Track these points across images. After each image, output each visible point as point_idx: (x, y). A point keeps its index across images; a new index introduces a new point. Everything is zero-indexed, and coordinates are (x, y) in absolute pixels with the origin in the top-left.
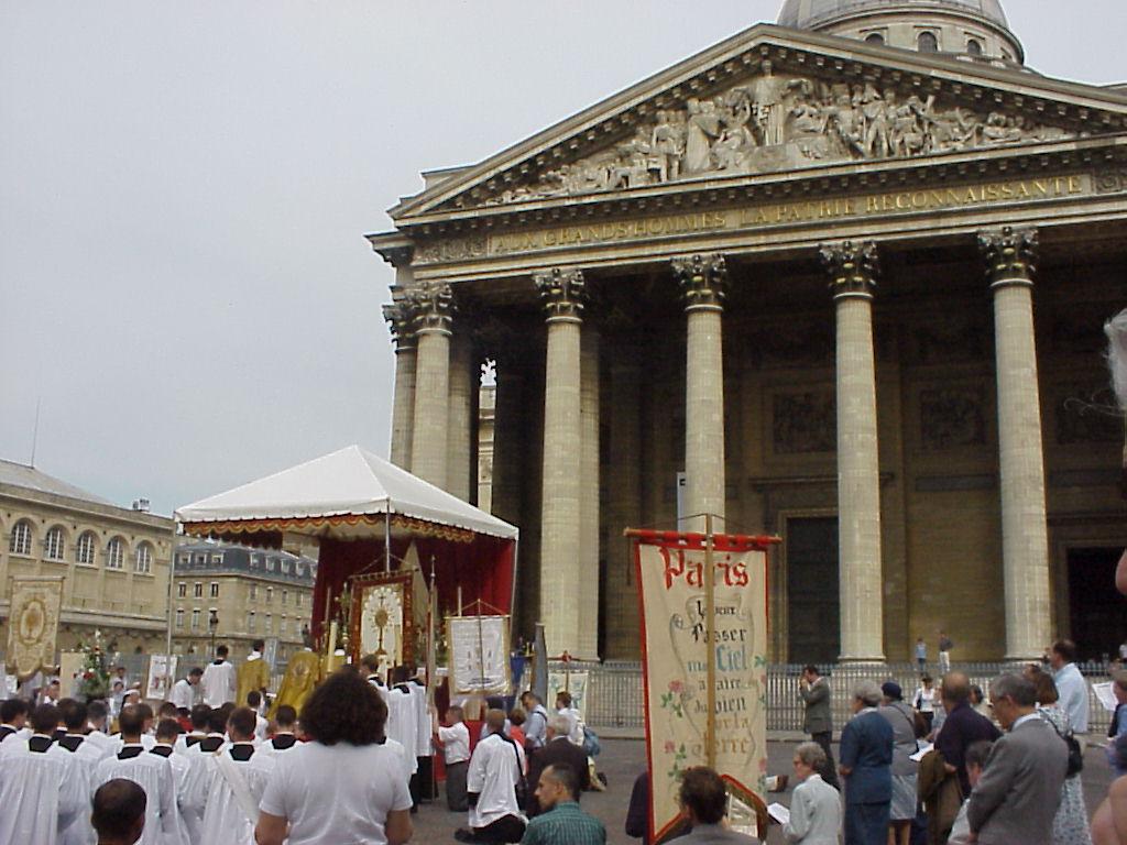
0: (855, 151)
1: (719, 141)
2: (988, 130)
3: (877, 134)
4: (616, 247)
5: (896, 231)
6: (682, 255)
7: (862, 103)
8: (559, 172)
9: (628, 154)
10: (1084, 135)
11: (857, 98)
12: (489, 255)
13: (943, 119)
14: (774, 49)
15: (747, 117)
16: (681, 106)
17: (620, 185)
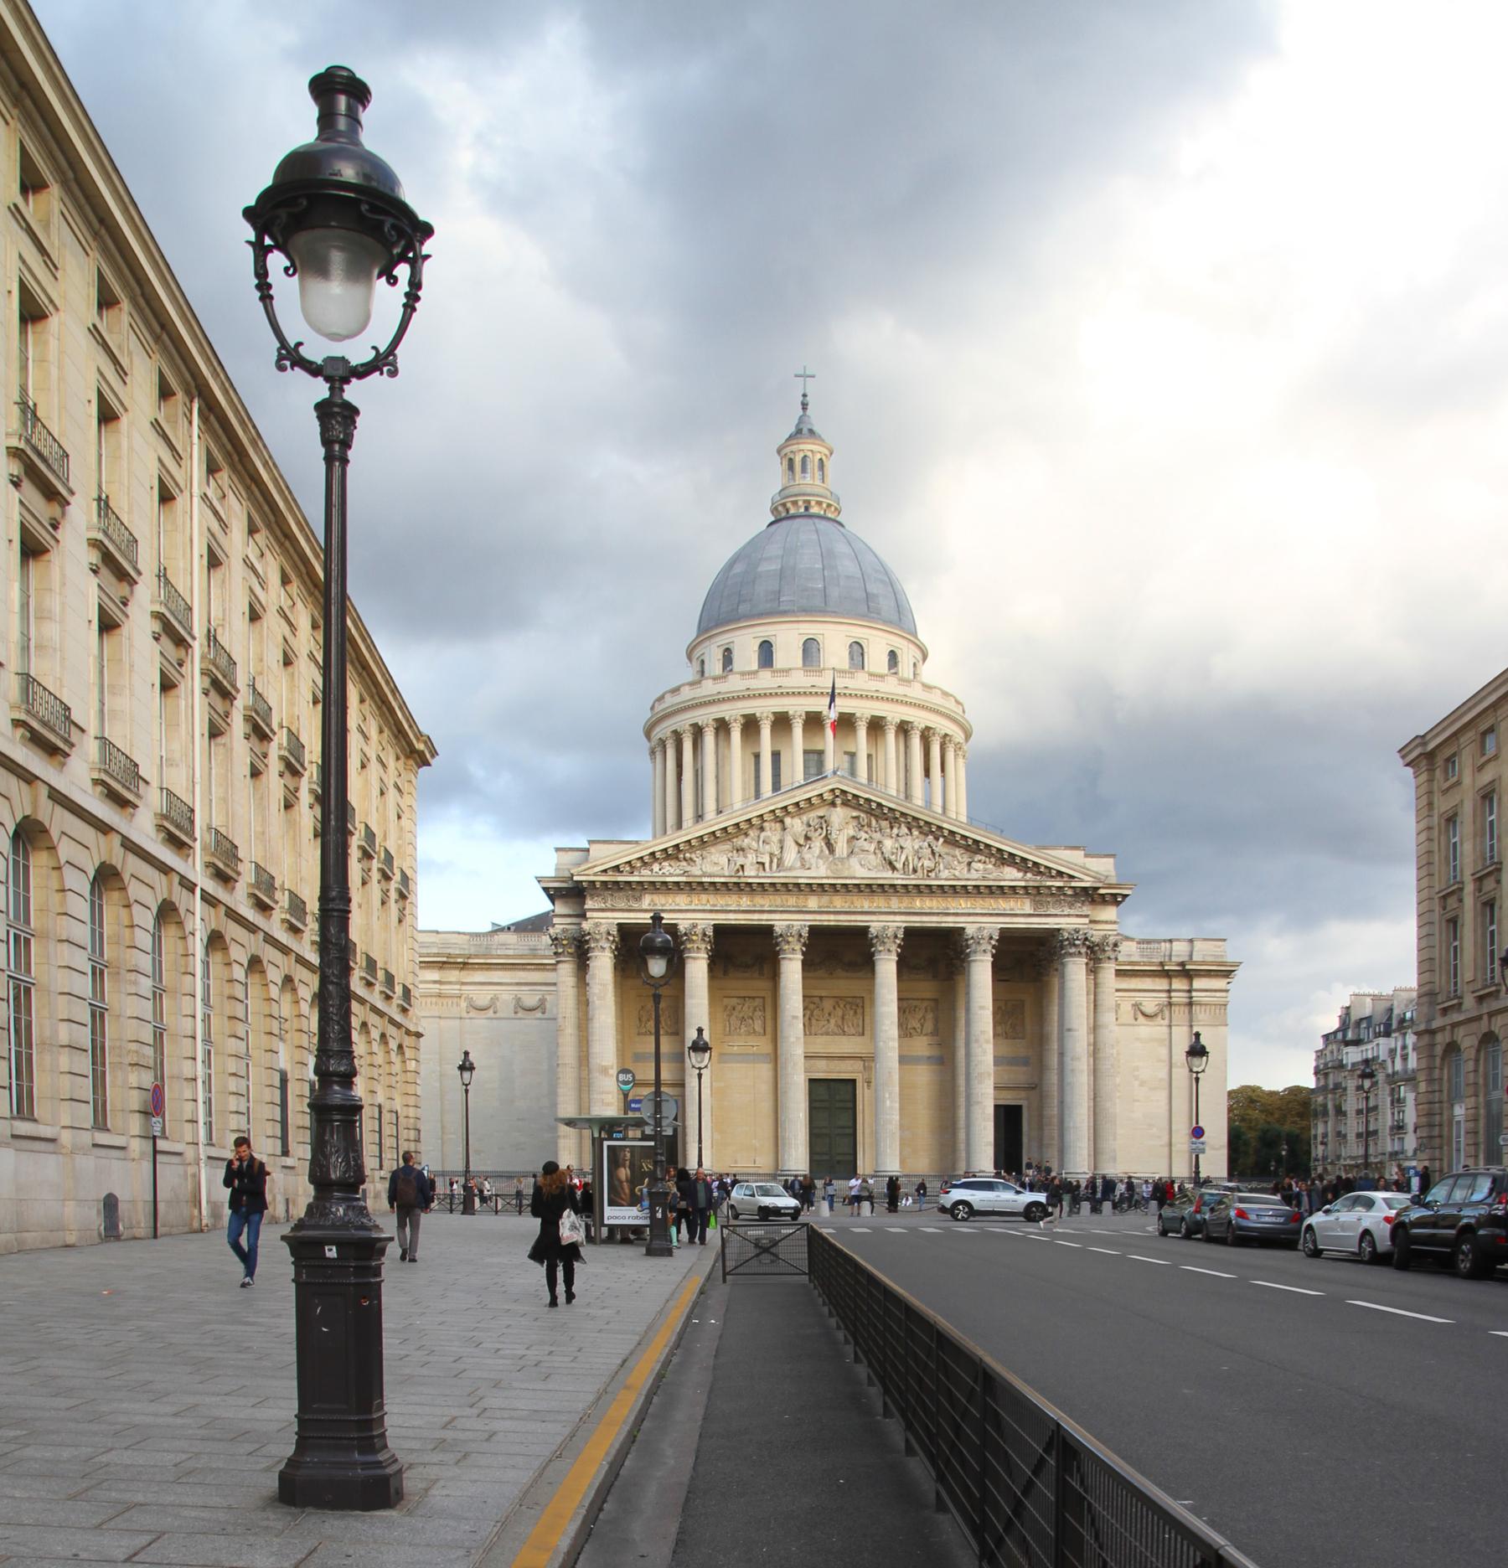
0: (894, 868)
2: (974, 865)
4: (735, 912)
5: (917, 921)
6: (780, 923)
10: (1029, 875)
11: (895, 831)
14: (844, 792)
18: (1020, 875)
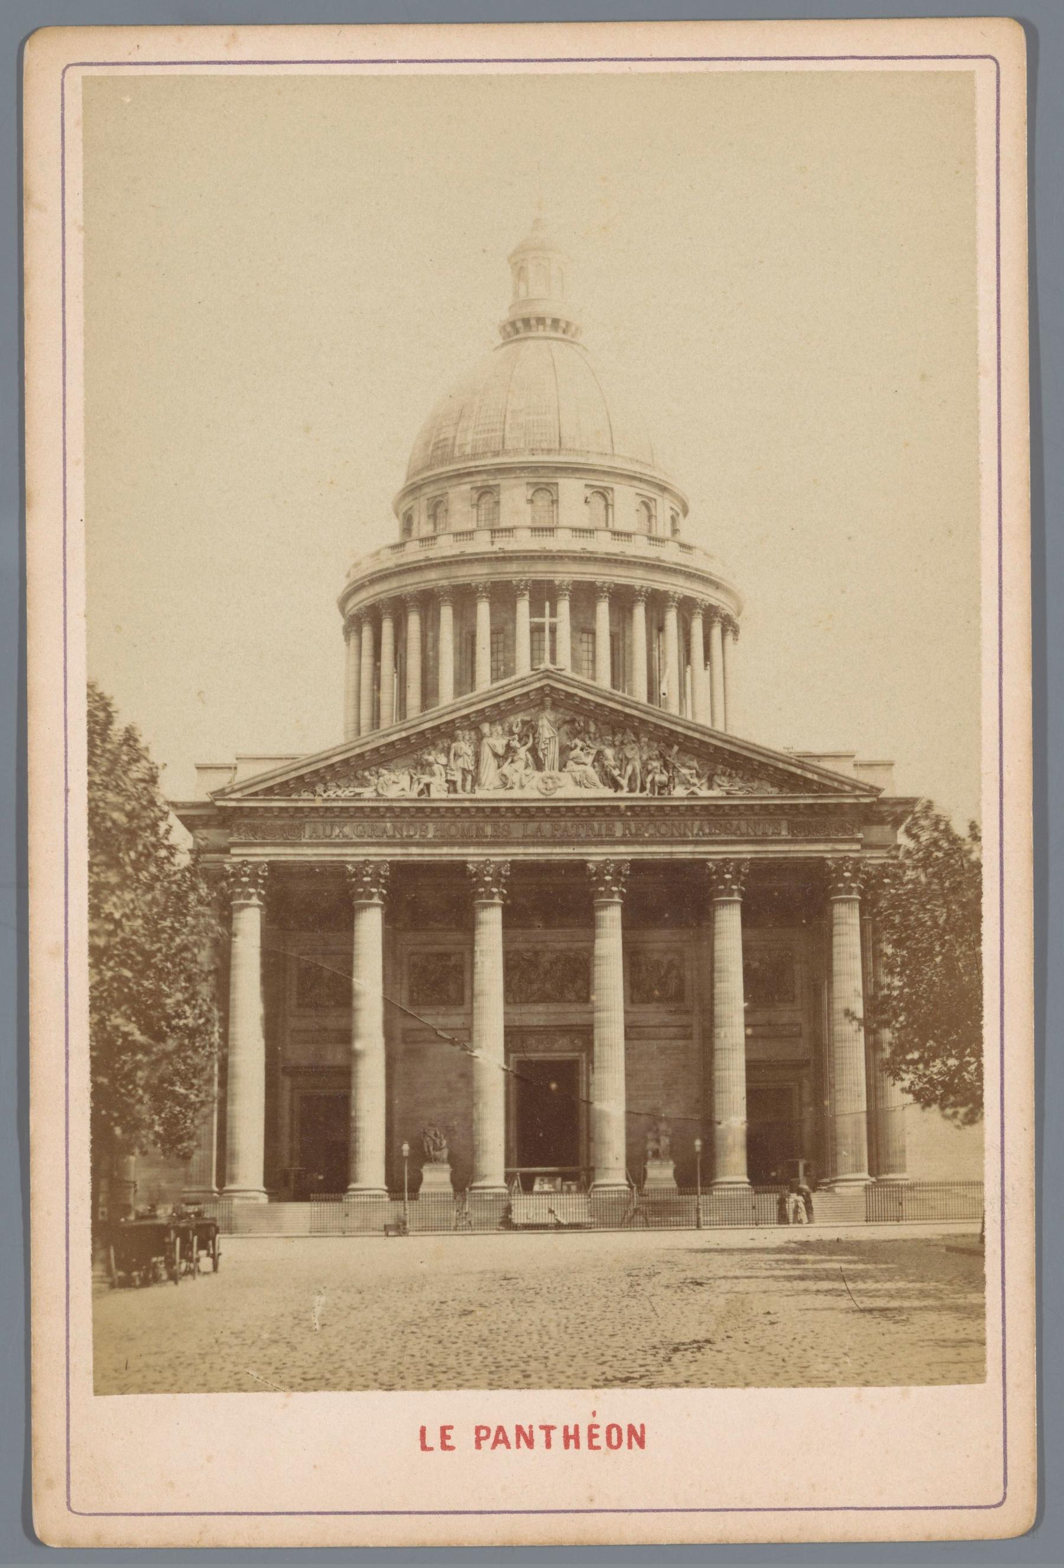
1: (506, 764)
2: (717, 779)
3: (634, 770)
7: (622, 743)
8: (367, 774)
9: (430, 765)
11: (619, 738)
12: (304, 840)
13: (683, 765)
15: (529, 745)
16: (475, 727)
17: (421, 792)
18: (774, 791)
